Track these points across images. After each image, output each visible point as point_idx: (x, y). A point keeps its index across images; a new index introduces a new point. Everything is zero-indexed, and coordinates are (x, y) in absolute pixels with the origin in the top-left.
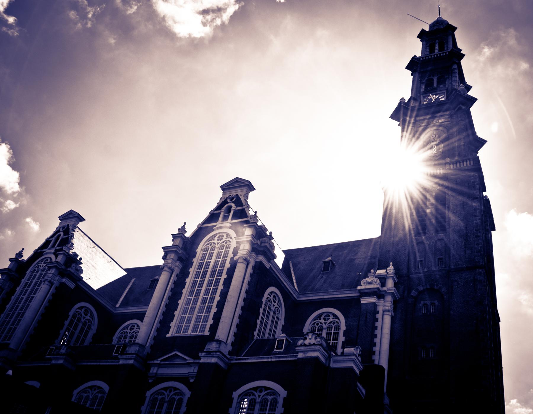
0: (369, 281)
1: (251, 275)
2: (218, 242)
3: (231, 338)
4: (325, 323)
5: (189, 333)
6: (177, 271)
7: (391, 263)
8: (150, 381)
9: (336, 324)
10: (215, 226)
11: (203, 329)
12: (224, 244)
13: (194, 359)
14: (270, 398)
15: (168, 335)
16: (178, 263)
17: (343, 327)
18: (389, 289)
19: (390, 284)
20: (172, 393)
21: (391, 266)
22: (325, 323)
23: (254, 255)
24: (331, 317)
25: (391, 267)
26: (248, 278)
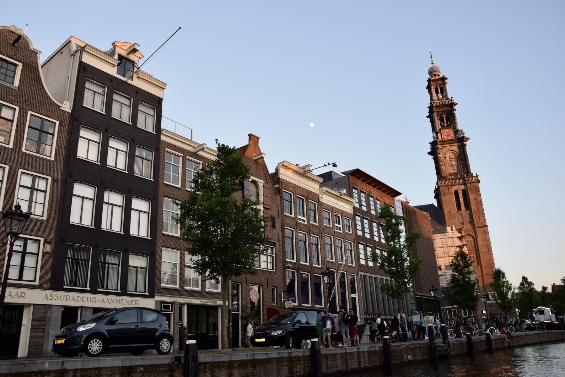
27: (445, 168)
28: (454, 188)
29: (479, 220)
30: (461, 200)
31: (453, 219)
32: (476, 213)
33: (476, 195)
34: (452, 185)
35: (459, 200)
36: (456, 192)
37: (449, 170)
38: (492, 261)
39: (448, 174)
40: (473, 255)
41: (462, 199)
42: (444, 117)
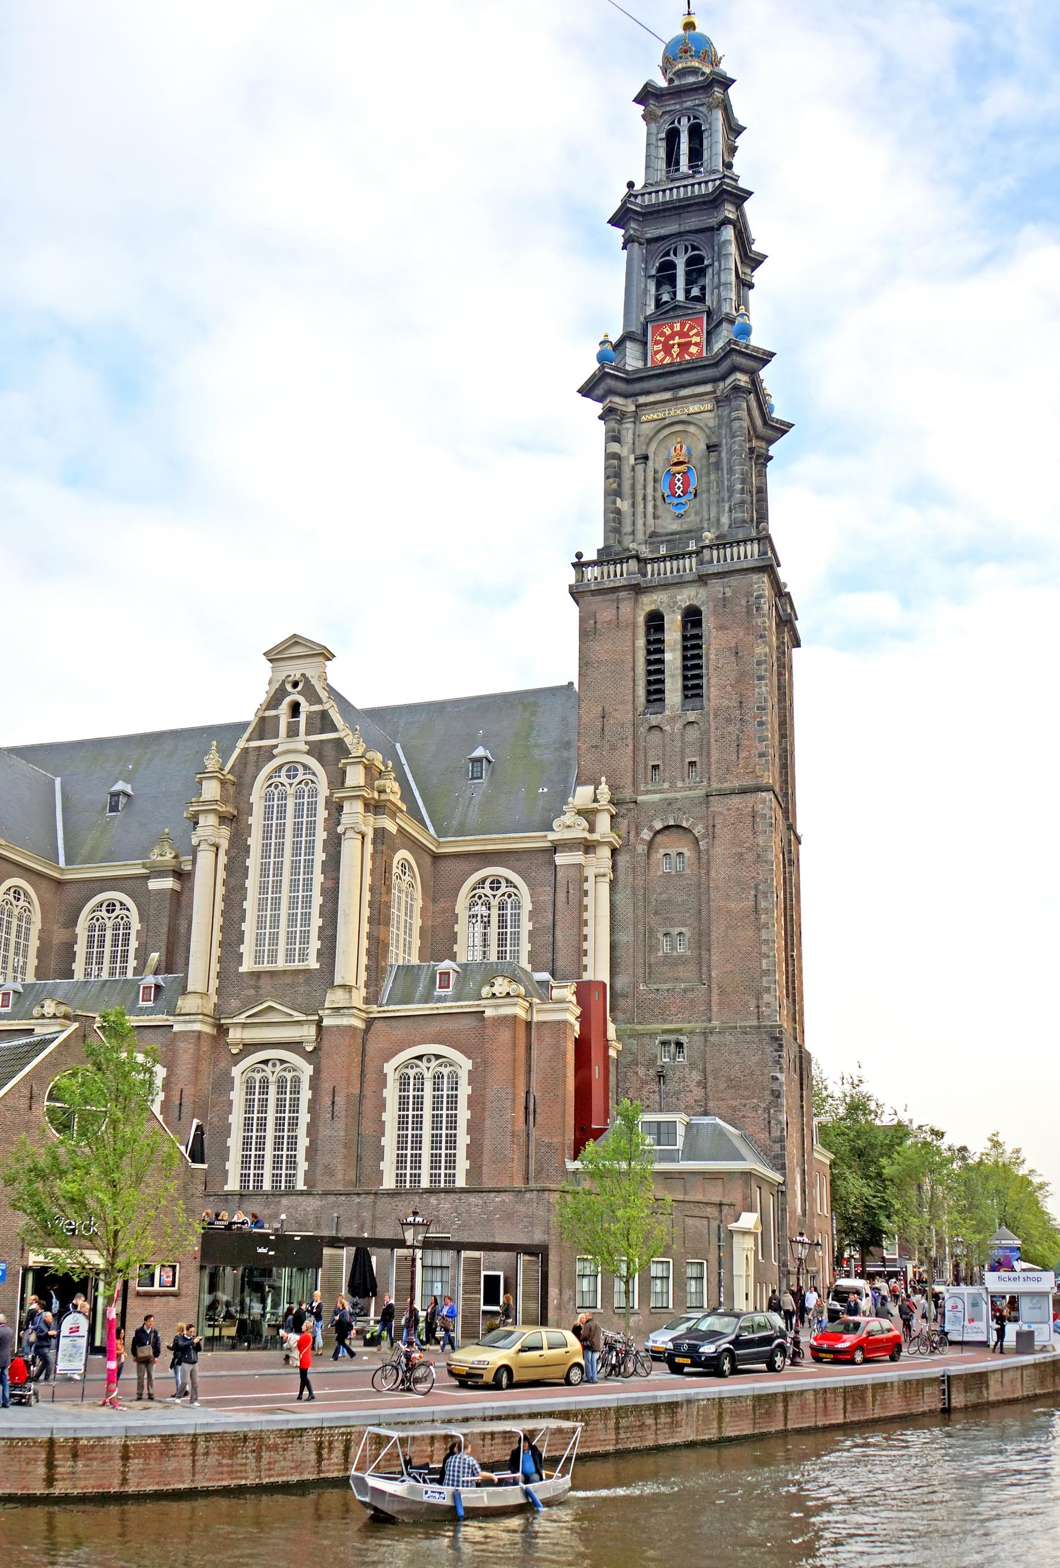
0: (568, 823)
1: (373, 857)
2: (291, 781)
3: (363, 976)
4: (494, 896)
5: (281, 964)
6: (224, 845)
7: (603, 779)
8: (235, 1051)
9: (513, 897)
10: (276, 746)
11: (303, 957)
12: (303, 785)
13: (307, 1015)
14: (445, 1071)
15: (241, 969)
16: (225, 831)
17: (527, 905)
18: (603, 836)
19: (603, 822)
20: (279, 1068)
21: (603, 784)
22: (494, 896)
23: (371, 817)
24: (504, 884)
25: (604, 788)
26: (368, 864)
27: (633, 505)
28: (649, 602)
29: (734, 757)
30: (673, 658)
31: (613, 748)
32: (729, 721)
33: (741, 634)
34: (637, 590)
35: (661, 661)
36: (655, 622)
37: (655, 517)
38: (764, 961)
39: (640, 536)
40: (684, 930)
41: (678, 655)
42: (680, 262)
